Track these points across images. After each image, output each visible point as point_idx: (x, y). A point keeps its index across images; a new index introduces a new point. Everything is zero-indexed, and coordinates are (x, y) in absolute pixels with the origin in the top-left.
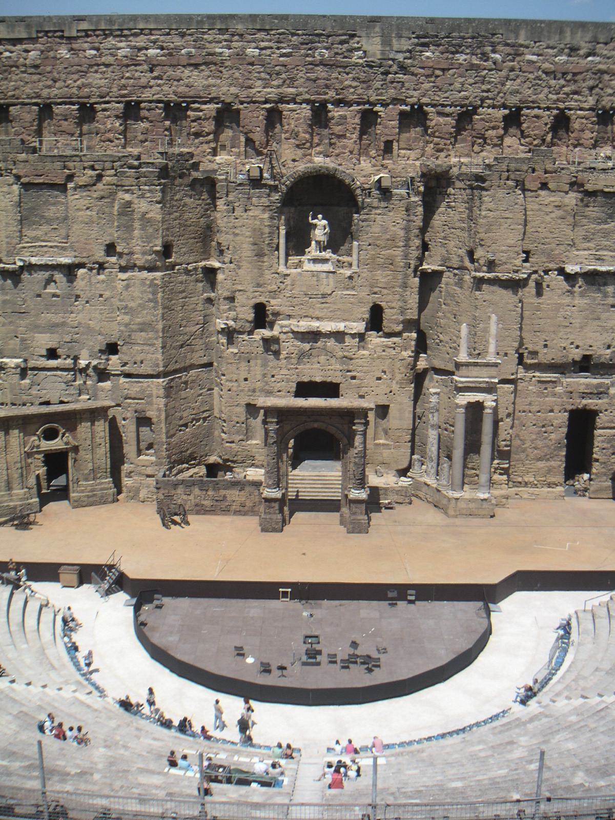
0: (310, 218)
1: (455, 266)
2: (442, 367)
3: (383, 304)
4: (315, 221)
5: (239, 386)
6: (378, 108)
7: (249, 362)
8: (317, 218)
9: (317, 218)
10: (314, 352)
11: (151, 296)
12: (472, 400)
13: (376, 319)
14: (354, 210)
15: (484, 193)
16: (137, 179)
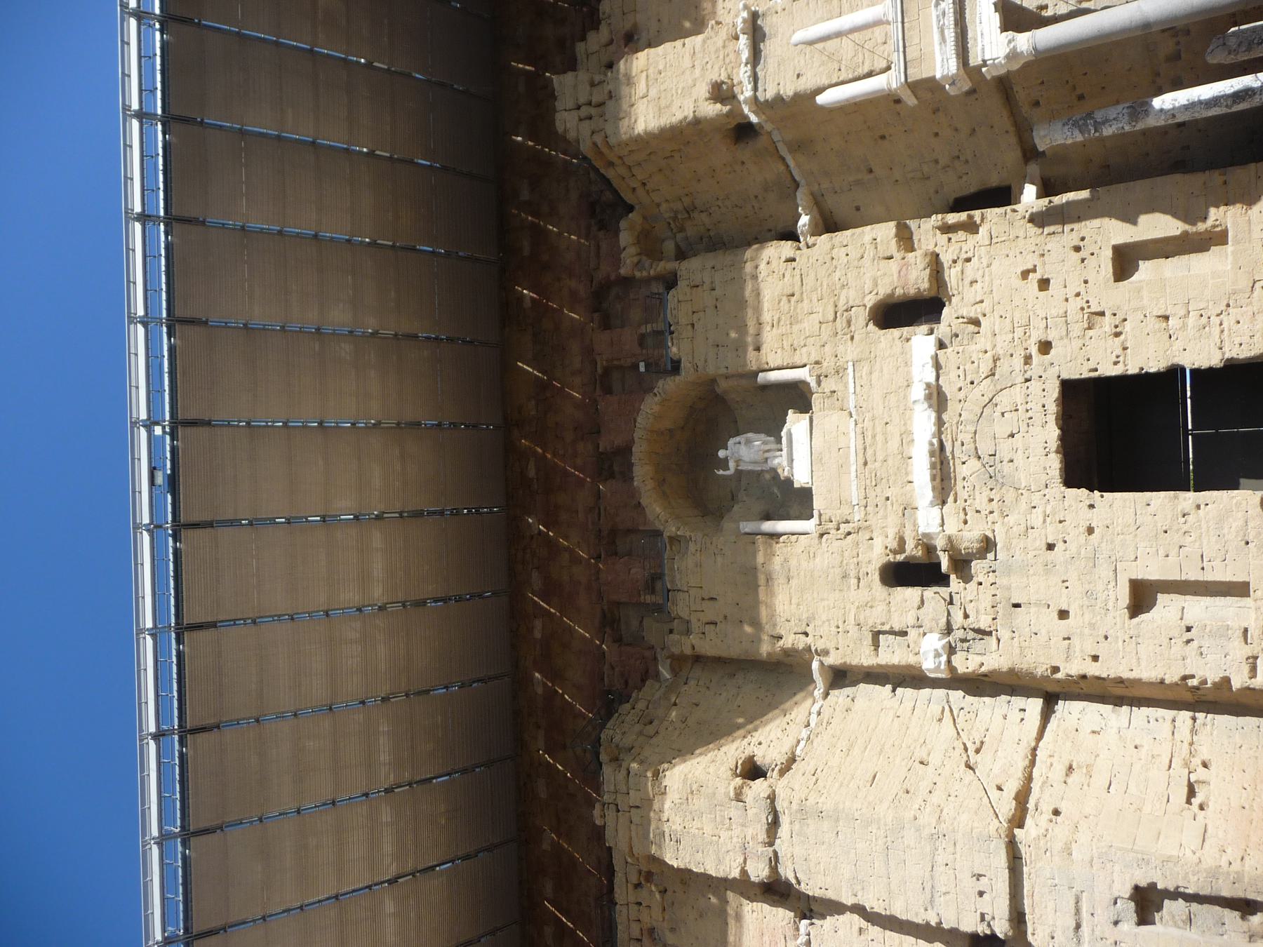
0: (727, 473)
1: (782, 168)
2: (1012, 139)
3: (870, 301)
4: (732, 464)
5: (1082, 634)
6: (600, 371)
7: (1017, 606)
8: (726, 460)
9: (726, 460)
10: (985, 448)
11: (826, 825)
12: (995, 19)
13: (906, 312)
14: (719, 391)
15: (612, 141)
16: (618, 811)
